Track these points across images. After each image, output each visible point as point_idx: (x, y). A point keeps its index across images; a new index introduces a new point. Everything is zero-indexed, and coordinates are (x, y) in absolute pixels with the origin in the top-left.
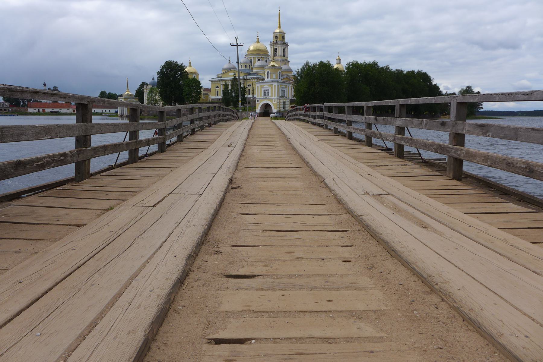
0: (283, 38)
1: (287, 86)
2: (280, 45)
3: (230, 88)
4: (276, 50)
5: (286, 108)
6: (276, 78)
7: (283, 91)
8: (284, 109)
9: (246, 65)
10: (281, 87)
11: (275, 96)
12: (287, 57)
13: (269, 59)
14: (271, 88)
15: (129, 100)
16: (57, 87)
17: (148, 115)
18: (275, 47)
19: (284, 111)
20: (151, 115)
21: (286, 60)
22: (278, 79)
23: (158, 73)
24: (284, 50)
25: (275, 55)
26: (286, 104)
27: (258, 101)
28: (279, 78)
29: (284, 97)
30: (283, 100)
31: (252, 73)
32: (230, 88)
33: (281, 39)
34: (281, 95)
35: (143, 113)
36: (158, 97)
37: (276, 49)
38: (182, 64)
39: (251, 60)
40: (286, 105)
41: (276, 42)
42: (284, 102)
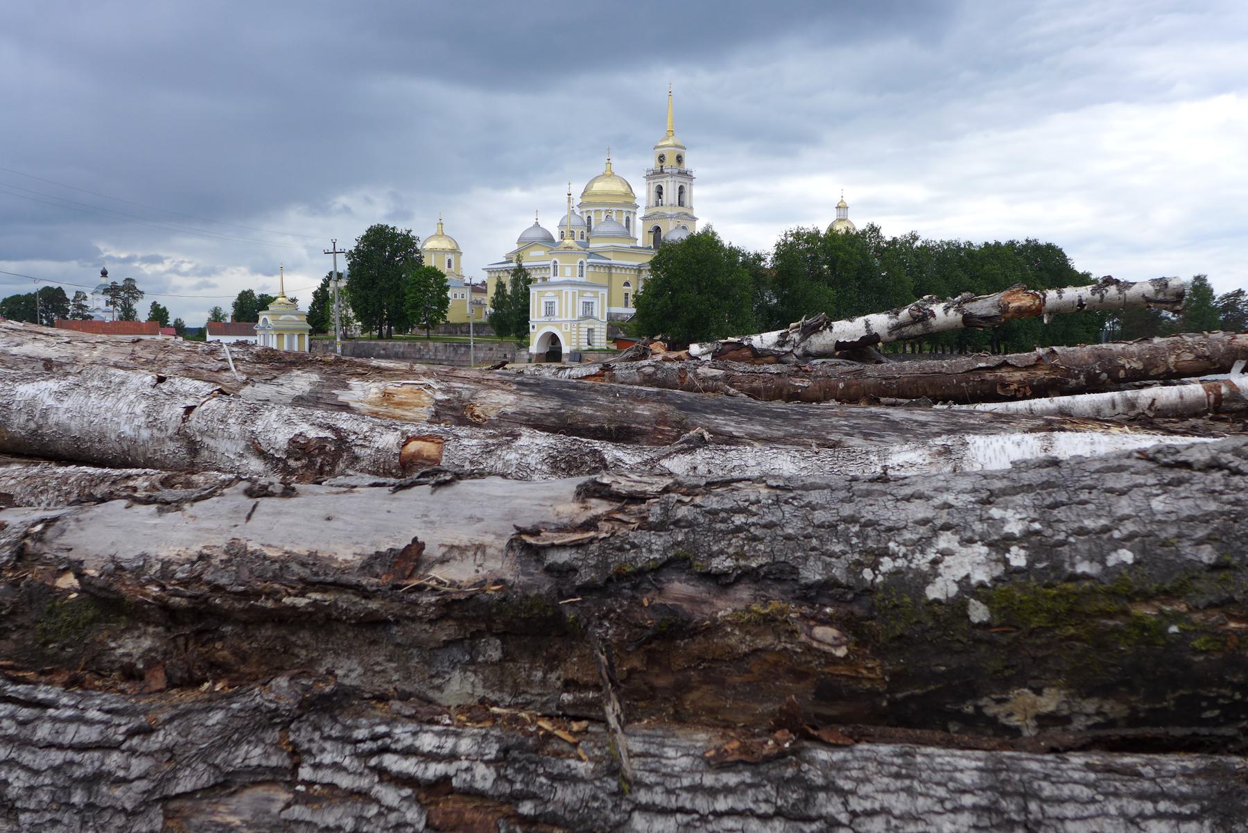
0: (679, 159)
2: (669, 179)
3: (509, 289)
4: (660, 191)
6: (573, 274)
8: (589, 344)
11: (566, 316)
12: (691, 208)
13: (635, 213)
14: (560, 298)
15: (282, 318)
16: (133, 280)
18: (659, 181)
19: (590, 350)
21: (686, 214)
22: (578, 279)
24: (681, 189)
25: (657, 205)
27: (533, 327)
32: (509, 289)
34: (581, 314)
35: (313, 349)
36: (351, 313)
37: (660, 188)
39: (589, 217)
41: (662, 171)
42: (590, 331)
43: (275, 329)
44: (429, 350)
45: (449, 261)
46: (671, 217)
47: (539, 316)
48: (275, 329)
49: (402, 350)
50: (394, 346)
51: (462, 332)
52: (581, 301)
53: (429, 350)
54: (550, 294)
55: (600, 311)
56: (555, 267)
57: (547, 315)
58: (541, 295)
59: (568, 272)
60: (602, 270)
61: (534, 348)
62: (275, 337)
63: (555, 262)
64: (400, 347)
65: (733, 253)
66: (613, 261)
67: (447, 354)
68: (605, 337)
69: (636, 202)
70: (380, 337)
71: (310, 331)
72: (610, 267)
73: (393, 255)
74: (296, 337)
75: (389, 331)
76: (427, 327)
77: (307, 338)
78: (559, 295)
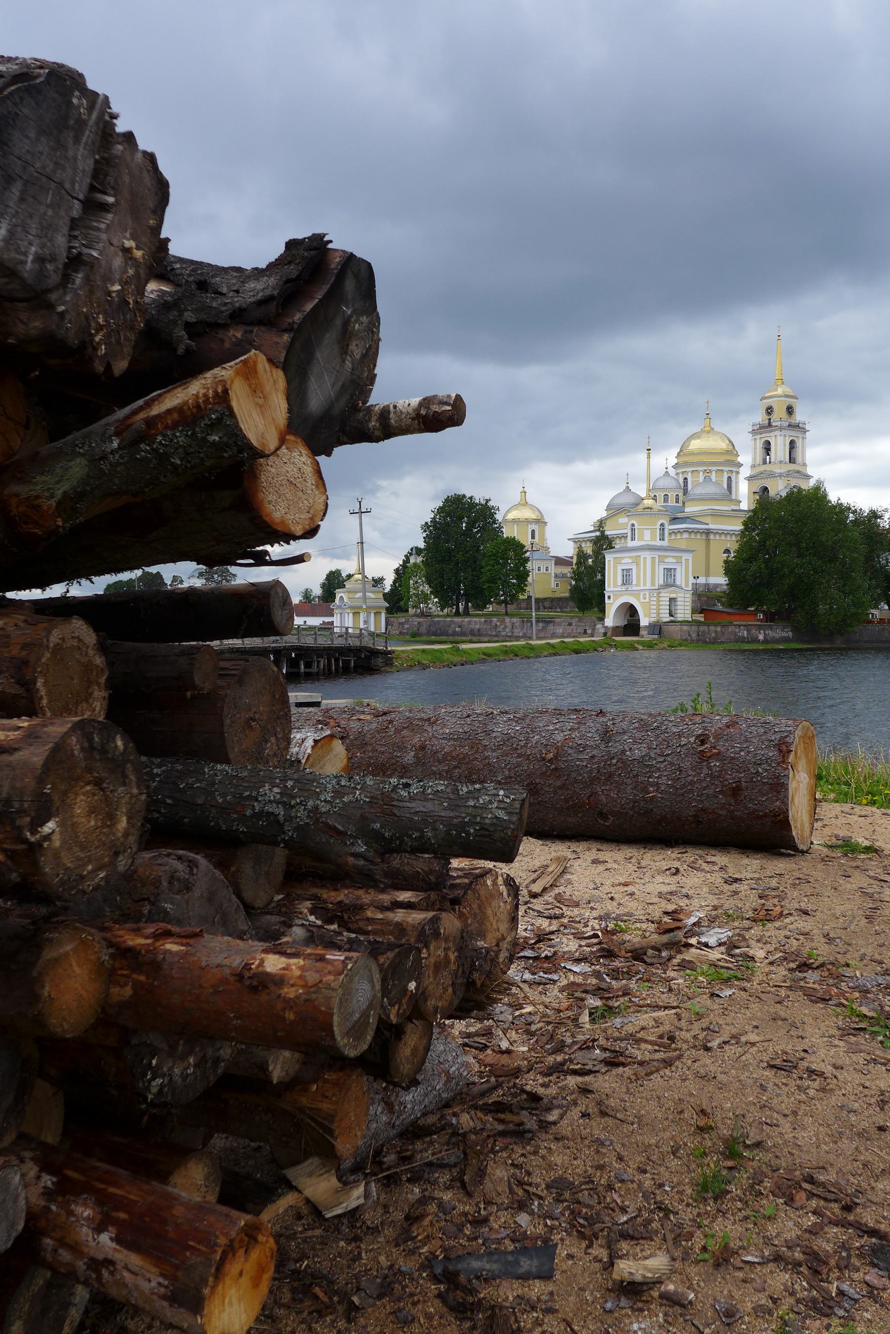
0: (790, 410)
1: (683, 559)
2: (778, 433)
5: (679, 615)
6: (653, 538)
7: (669, 572)
8: (671, 615)
9: (666, 495)
10: (661, 561)
11: (645, 585)
12: (805, 465)
13: (738, 473)
14: (638, 565)
17: (401, 633)
18: (766, 436)
20: (407, 634)
21: (798, 472)
22: (659, 543)
23: (426, 527)
24: (792, 444)
25: (765, 462)
26: (679, 603)
27: (609, 597)
28: (662, 539)
29: (673, 585)
30: (667, 595)
31: (679, 515)
33: (784, 414)
34: (662, 582)
35: (389, 627)
36: (427, 589)
38: (487, 501)
39: (686, 479)
40: (679, 607)
41: (770, 425)
43: (351, 608)
44: (506, 627)
45: (533, 532)
46: (781, 475)
47: (615, 585)
48: (351, 608)
49: (477, 627)
50: (470, 622)
51: (545, 608)
52: (662, 567)
53: (506, 627)
54: (627, 561)
55: (685, 579)
56: (633, 530)
57: (624, 584)
58: (617, 561)
59: (647, 536)
60: (698, 536)
61: (609, 621)
62: (351, 615)
63: (633, 525)
64: (476, 623)
65: (841, 510)
66: (711, 526)
67: (525, 631)
68: (689, 608)
69: (740, 459)
70: (457, 614)
71: (387, 609)
72: (708, 532)
73: (471, 526)
74: (372, 615)
75: (466, 608)
76: (505, 602)
77: (383, 616)
78: (636, 561)
